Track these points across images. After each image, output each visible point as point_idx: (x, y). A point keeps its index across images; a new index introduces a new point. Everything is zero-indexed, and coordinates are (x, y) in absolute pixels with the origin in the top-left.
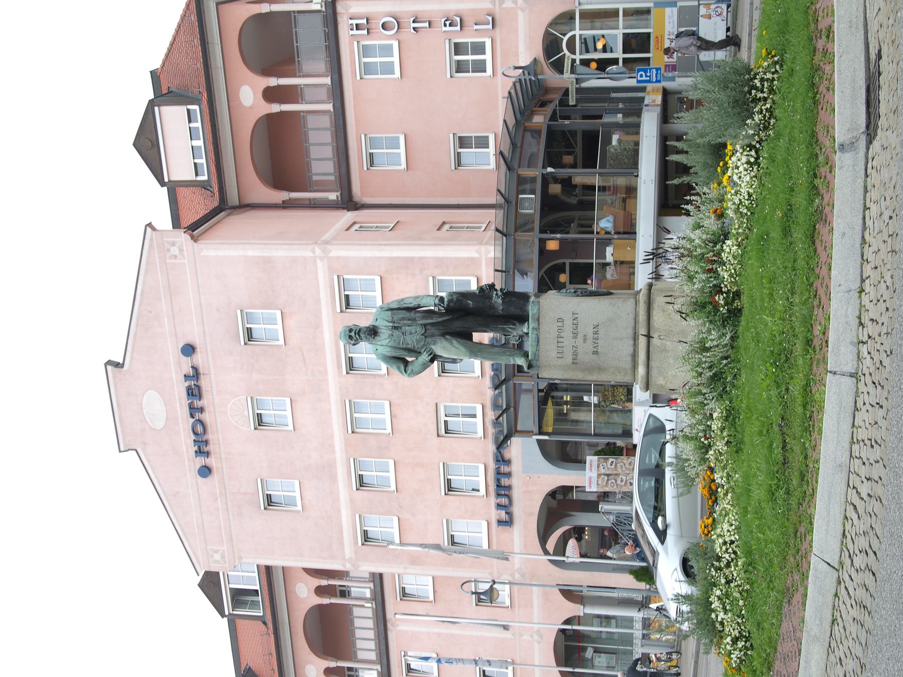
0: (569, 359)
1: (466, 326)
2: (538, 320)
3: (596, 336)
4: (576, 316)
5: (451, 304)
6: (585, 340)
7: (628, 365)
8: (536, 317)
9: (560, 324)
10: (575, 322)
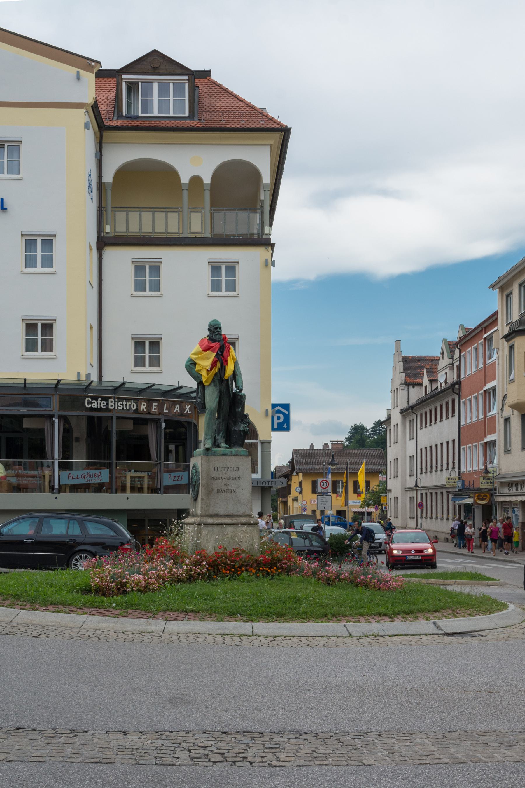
0: (214, 474)
1: (225, 406)
2: (237, 455)
3: (229, 491)
4: (241, 479)
5: (239, 397)
6: (226, 485)
7: (211, 512)
8: (239, 454)
9: (235, 469)
10: (237, 478)
